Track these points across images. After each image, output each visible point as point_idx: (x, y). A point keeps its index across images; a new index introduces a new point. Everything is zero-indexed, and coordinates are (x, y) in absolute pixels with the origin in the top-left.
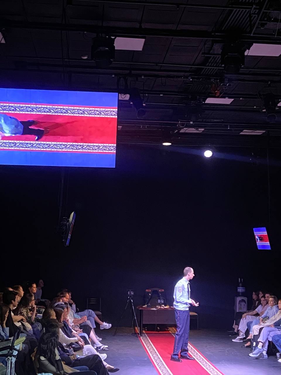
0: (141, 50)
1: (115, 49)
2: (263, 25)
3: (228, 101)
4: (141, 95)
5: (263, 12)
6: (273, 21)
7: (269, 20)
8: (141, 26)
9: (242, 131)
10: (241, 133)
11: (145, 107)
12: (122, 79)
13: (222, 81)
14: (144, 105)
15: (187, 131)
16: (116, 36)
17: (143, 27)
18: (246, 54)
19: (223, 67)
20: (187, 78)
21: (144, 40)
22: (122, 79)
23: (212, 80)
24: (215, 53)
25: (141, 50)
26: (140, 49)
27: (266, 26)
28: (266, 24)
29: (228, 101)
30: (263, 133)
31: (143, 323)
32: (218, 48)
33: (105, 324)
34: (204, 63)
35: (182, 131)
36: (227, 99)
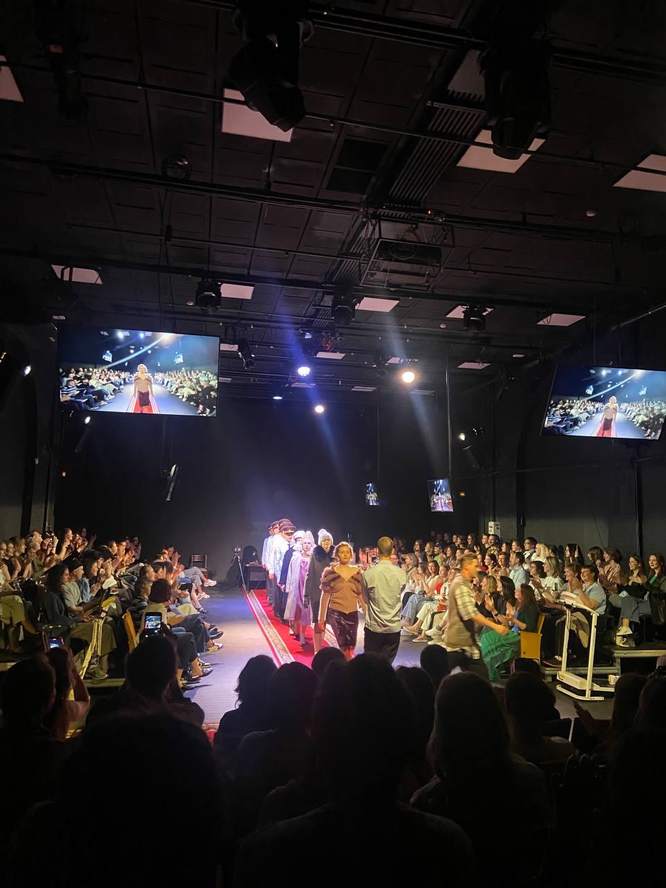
0: (250, 298)
1: (223, 295)
2: (372, 275)
3: (338, 356)
4: (251, 346)
5: (373, 261)
6: (382, 271)
7: (378, 269)
8: (249, 273)
9: (353, 387)
10: (353, 389)
11: (255, 359)
12: (230, 328)
13: (333, 335)
14: (253, 356)
15: (299, 386)
16: (222, 282)
17: (251, 274)
18: (356, 308)
19: (332, 320)
20: (298, 330)
21: (252, 288)
22: (230, 328)
23: (323, 333)
24: (326, 305)
25: (250, 298)
26: (249, 297)
27: (375, 277)
28: (375, 274)
29: (338, 356)
30: (374, 391)
31: (251, 580)
32: (328, 301)
33: (210, 581)
34: (314, 316)
35: (293, 386)
36: (338, 353)
